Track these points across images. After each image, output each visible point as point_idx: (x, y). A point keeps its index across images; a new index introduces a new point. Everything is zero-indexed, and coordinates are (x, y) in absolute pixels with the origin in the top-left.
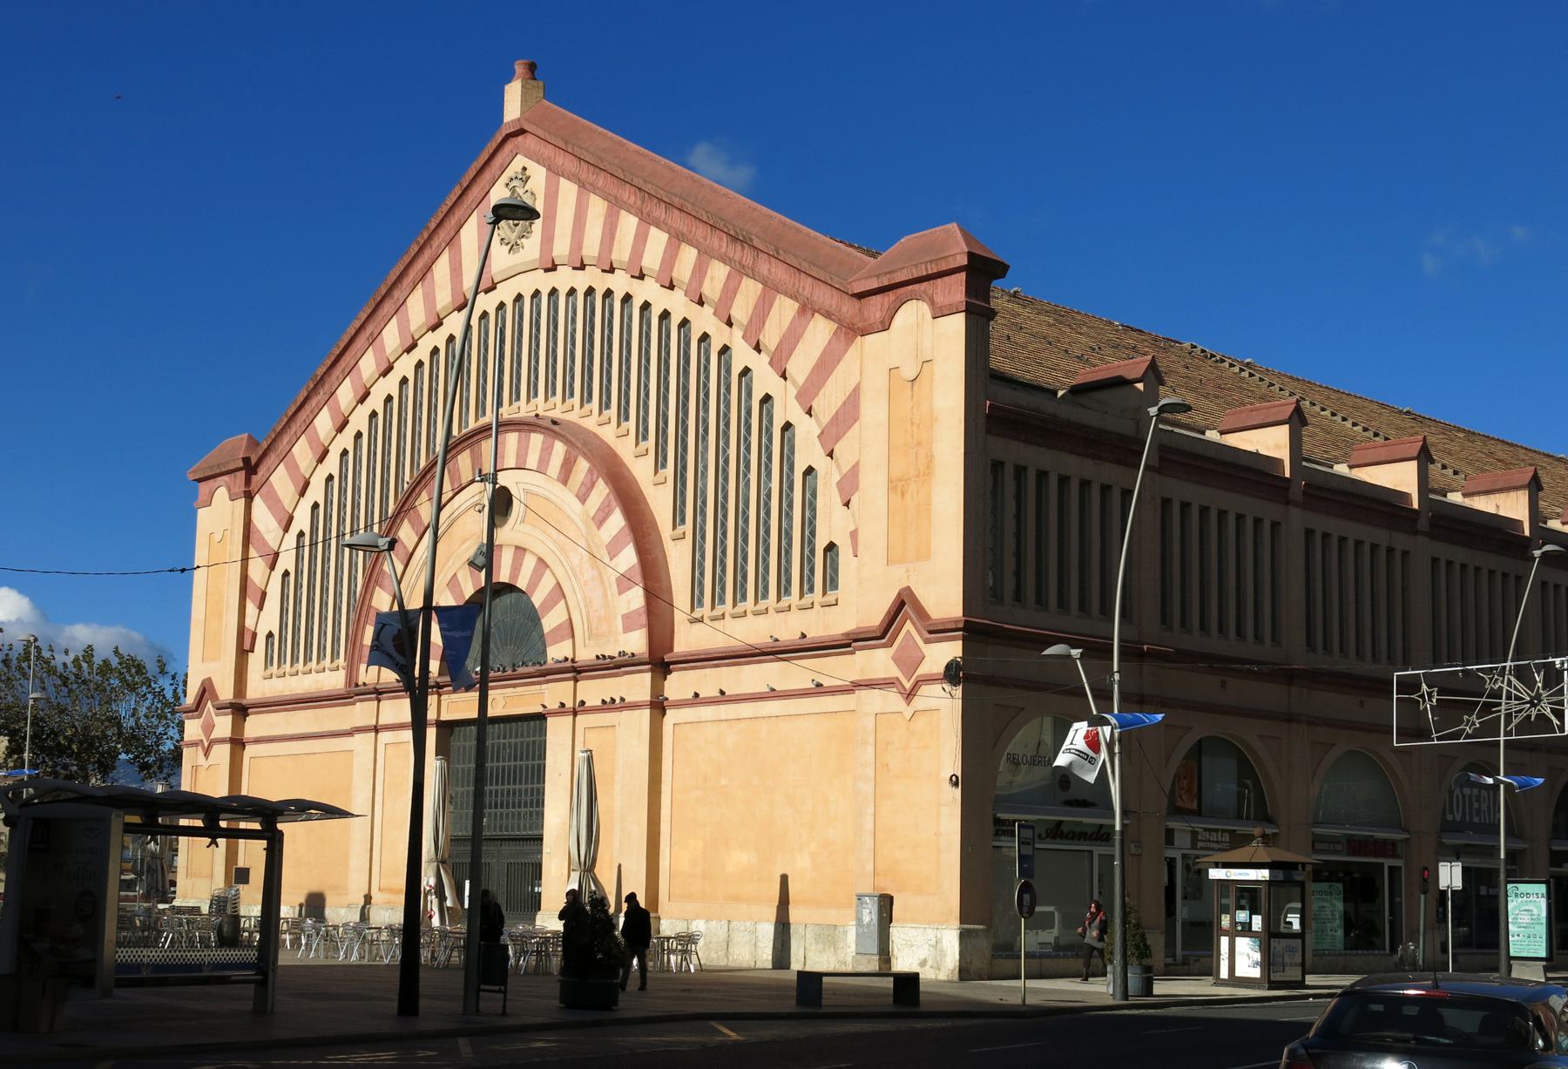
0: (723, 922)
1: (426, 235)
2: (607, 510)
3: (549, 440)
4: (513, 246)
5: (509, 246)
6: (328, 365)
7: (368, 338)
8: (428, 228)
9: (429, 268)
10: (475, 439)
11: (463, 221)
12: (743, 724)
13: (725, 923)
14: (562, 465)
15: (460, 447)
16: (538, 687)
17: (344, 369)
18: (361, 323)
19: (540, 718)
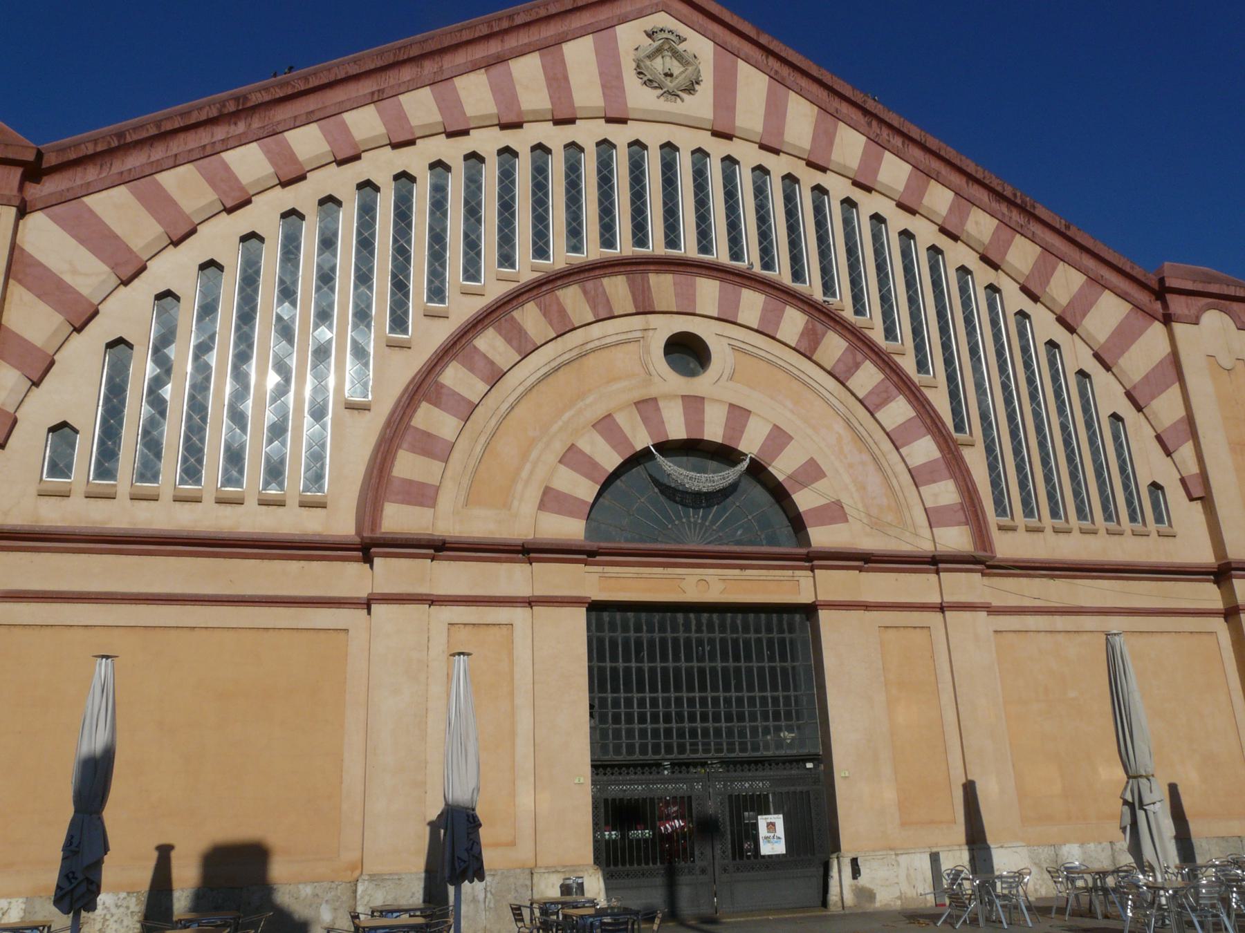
0: (1105, 844)
1: (505, 24)
2: (884, 395)
3: (775, 303)
4: (665, 92)
5: (661, 92)
6: (277, 96)
7: (373, 93)
8: (511, 17)
9: (501, 60)
10: (641, 268)
11: (569, 37)
12: (1085, 637)
13: (1106, 844)
14: (802, 334)
15: (616, 269)
16: (790, 572)
17: (312, 112)
18: (358, 72)
19: (809, 611)
